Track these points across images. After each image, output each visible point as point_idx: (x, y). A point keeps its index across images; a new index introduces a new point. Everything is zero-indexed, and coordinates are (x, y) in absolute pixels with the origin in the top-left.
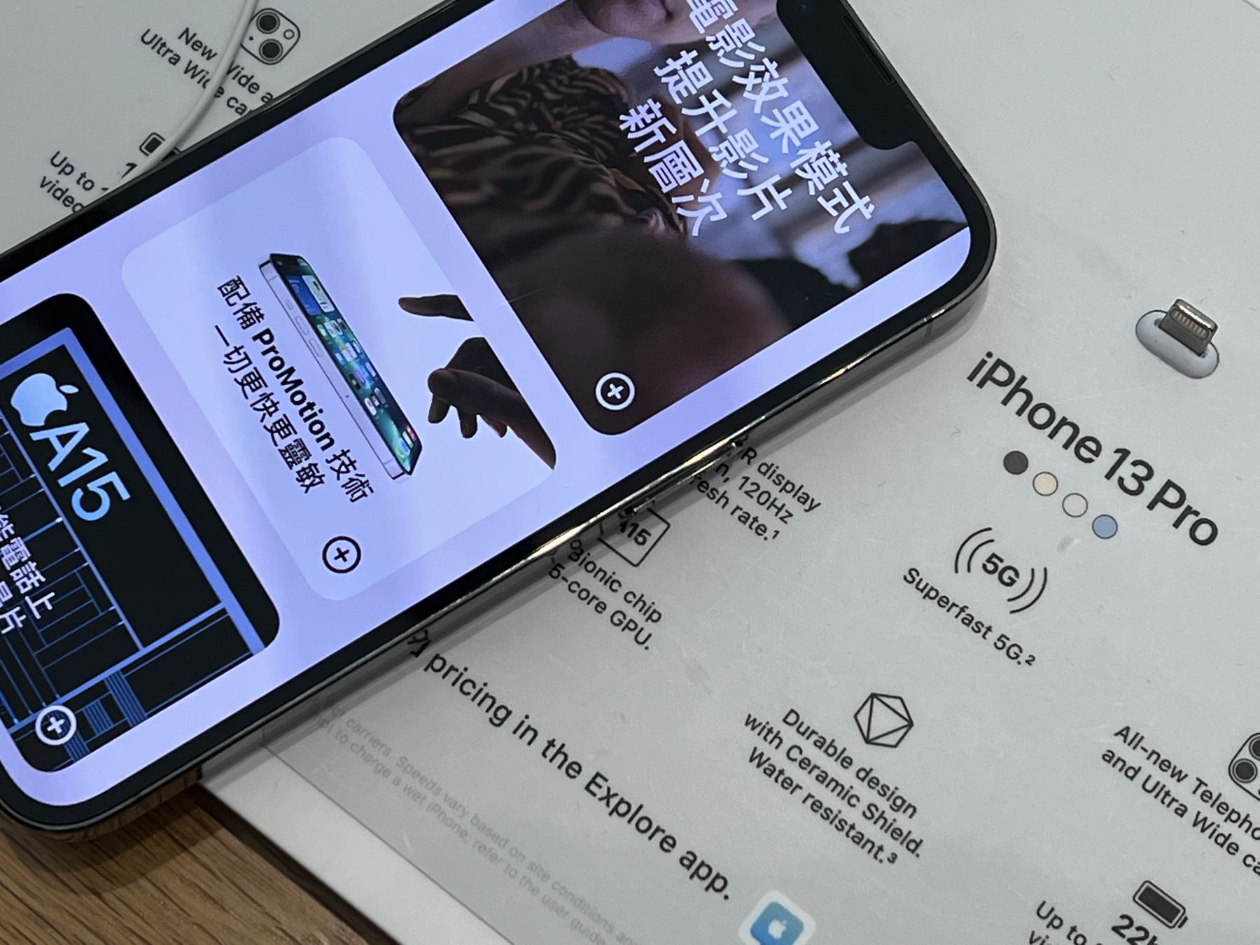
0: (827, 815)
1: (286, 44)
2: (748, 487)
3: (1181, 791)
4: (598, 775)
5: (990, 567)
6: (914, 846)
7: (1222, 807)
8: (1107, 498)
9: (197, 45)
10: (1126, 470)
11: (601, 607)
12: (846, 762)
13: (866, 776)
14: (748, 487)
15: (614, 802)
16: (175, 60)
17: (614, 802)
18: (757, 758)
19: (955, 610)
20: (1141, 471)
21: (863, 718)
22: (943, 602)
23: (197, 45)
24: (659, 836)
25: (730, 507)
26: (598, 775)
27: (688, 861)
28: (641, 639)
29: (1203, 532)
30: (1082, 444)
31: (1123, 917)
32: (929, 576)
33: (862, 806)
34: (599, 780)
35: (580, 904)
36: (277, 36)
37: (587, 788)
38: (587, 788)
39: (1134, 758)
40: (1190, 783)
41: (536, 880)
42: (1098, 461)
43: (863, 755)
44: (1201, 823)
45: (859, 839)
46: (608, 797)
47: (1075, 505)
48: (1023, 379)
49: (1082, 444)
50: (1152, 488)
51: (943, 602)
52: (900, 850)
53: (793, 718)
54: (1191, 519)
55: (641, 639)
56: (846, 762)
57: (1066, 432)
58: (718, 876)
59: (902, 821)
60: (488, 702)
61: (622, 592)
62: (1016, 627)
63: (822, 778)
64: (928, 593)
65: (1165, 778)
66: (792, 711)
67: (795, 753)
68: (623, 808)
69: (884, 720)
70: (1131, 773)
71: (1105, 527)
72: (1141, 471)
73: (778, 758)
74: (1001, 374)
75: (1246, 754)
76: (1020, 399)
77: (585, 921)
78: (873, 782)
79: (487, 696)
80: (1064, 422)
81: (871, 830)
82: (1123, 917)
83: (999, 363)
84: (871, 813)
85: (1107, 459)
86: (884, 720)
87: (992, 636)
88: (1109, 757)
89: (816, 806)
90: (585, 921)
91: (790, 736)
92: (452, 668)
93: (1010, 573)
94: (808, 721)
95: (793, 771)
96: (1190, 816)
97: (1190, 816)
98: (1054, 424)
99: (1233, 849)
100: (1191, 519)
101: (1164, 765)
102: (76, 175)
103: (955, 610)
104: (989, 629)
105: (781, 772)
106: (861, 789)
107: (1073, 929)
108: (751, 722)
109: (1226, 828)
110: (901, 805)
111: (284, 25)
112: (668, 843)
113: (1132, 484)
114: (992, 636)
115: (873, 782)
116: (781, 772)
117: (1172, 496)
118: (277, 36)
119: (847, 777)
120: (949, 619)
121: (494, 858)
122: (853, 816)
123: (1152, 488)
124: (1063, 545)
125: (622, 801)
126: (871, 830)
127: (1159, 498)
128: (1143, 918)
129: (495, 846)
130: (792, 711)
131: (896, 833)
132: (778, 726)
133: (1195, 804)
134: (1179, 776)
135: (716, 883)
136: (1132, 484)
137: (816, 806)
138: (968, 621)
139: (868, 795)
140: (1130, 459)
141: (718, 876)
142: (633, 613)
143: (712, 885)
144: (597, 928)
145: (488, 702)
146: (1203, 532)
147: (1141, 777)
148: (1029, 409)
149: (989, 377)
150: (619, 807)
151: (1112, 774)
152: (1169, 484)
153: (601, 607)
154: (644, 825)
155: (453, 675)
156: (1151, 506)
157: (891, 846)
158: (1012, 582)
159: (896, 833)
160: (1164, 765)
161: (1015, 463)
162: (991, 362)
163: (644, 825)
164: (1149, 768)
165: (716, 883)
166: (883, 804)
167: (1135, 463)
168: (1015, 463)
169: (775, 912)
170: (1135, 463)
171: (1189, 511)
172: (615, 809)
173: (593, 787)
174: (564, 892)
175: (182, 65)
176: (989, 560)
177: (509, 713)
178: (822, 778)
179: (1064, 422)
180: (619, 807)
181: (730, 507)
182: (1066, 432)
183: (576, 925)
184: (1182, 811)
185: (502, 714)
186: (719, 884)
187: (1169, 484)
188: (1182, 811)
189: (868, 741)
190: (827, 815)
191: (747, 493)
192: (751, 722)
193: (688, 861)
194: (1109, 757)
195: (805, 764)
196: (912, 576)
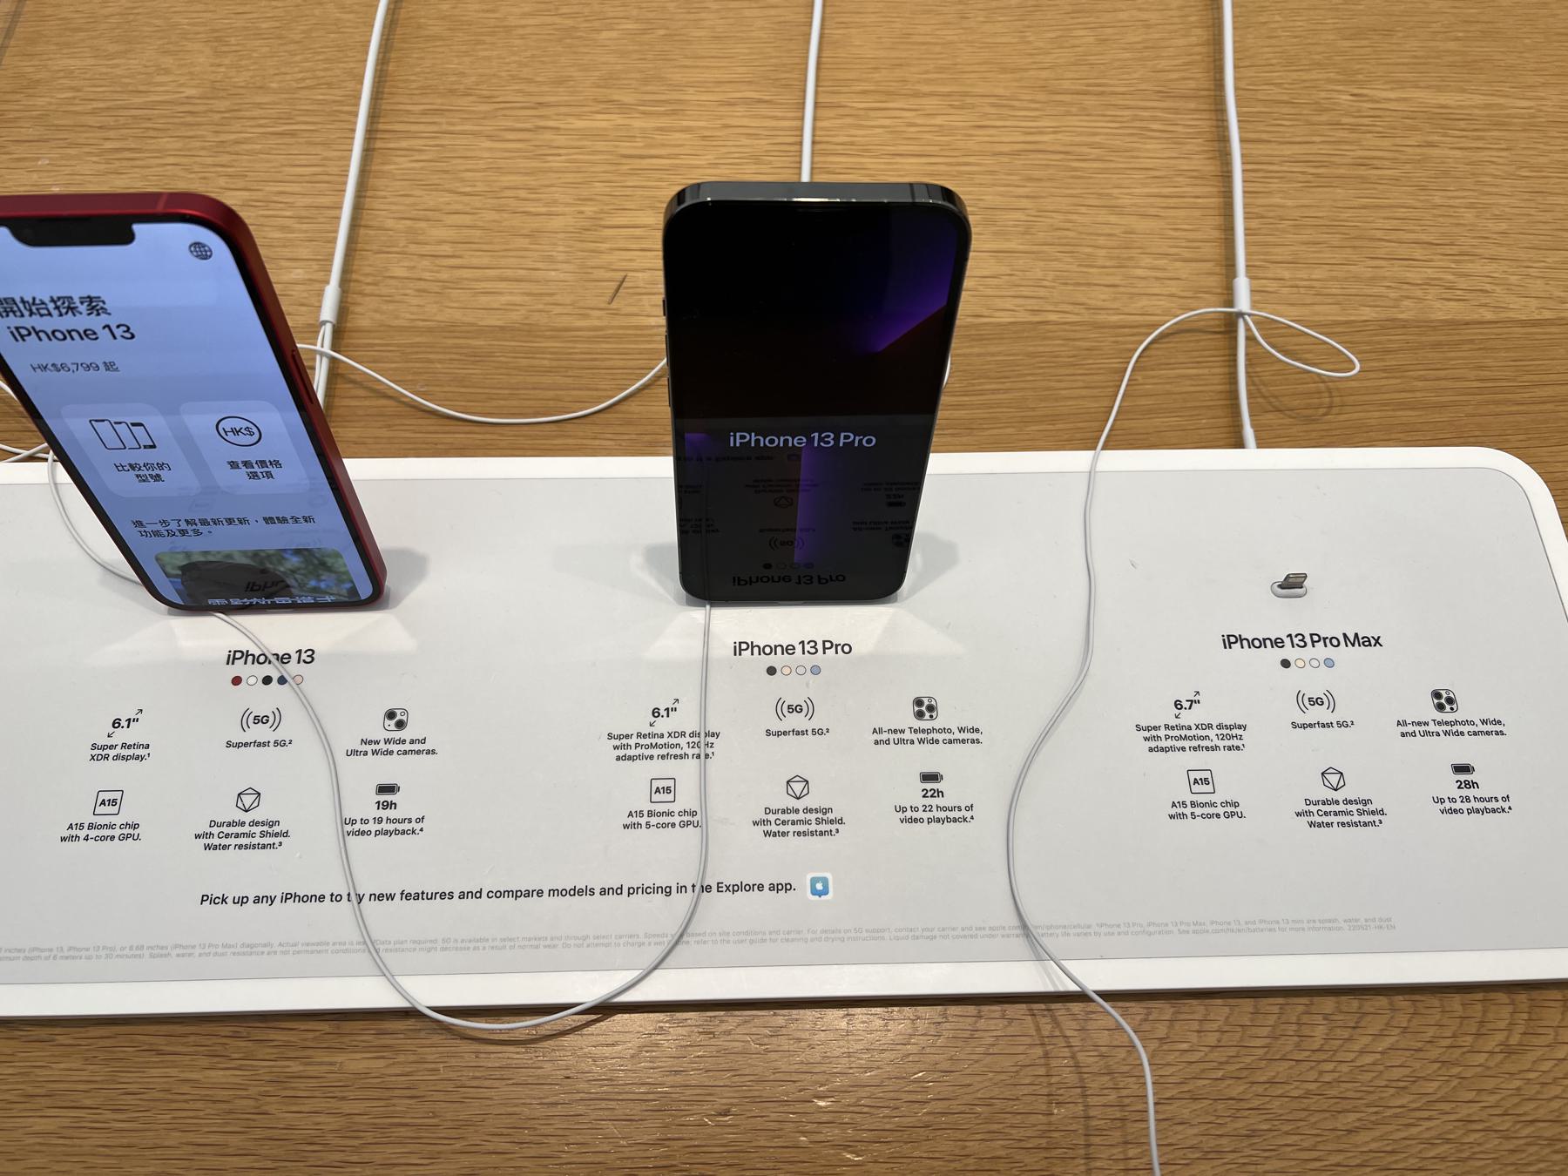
0: (805, 834)
1: (404, 718)
2: (691, 745)
3: (907, 735)
4: (718, 883)
5: (791, 710)
6: (841, 821)
7: (923, 731)
8: (809, 661)
9: (370, 742)
10: (807, 647)
11: (673, 825)
12: (797, 811)
13: (808, 810)
14: (691, 745)
15: (731, 888)
16: (366, 754)
17: (731, 888)
18: (767, 834)
19: (791, 733)
20: (812, 644)
21: (790, 792)
22: (785, 733)
23: (370, 742)
24: (756, 887)
25: (690, 757)
26: (718, 883)
27: (772, 887)
28: (696, 825)
29: (847, 649)
30: (787, 649)
31: (923, 791)
32: (774, 729)
33: (814, 822)
34: (720, 885)
35: (747, 933)
36: (398, 717)
37: (718, 891)
38: (718, 891)
39: (884, 736)
40: (908, 731)
41: (725, 938)
42: (796, 651)
43: (800, 804)
44: (921, 741)
45: (822, 834)
46: (728, 888)
47: (801, 670)
48: (752, 643)
49: (787, 649)
50: (820, 647)
51: (785, 733)
52: (838, 826)
53: (768, 811)
54: (839, 648)
55: (696, 825)
56: (797, 811)
57: (779, 649)
58: (786, 885)
59: (830, 816)
60: (660, 889)
61: (676, 814)
62: (816, 723)
63: (793, 823)
64: (778, 734)
65: (899, 735)
66: (766, 808)
67: (778, 822)
68: (736, 888)
69: (798, 787)
70: (887, 742)
71: (816, 670)
72: (812, 644)
73: (774, 828)
74: (744, 646)
75: (916, 709)
76: (756, 650)
77: (754, 937)
78: (811, 811)
79: (658, 888)
80: (776, 647)
81: (823, 827)
82: (923, 791)
83: (740, 643)
84: (818, 821)
85: (799, 648)
86: (798, 787)
87: (810, 732)
88: (877, 742)
89: (799, 834)
90: (754, 937)
91: (772, 817)
92: (638, 888)
93: (798, 708)
94: (773, 807)
95: (782, 828)
96: (916, 742)
97: (916, 742)
98: (774, 650)
99: (937, 741)
100: (839, 648)
101: (895, 731)
102: (359, 821)
103: (791, 733)
104: (807, 731)
105: (779, 832)
106: (809, 816)
107: (911, 807)
108: (755, 823)
109: (930, 736)
110: (826, 811)
111: (398, 712)
112: (760, 887)
113: (813, 650)
114: (810, 732)
115: (811, 811)
116: (779, 832)
117: (828, 645)
118: (398, 717)
119: (801, 816)
120: (791, 737)
121: (705, 942)
122: (813, 827)
123: (820, 647)
124: (807, 685)
125: (733, 886)
126: (823, 827)
127: (825, 649)
128: (929, 786)
129: (702, 938)
130: (766, 808)
131: (832, 822)
132: (765, 817)
133: (914, 737)
134: (902, 731)
135: (787, 887)
136: (813, 650)
137: (799, 834)
138: (798, 733)
139: (813, 816)
140: (806, 643)
141: (786, 885)
142: (686, 818)
143: (786, 889)
144: (760, 937)
145: (660, 889)
146: (847, 649)
147: (891, 741)
148: (761, 651)
149: (741, 650)
150: (734, 889)
151: (882, 747)
152: (824, 642)
153: (673, 825)
154: (747, 888)
155: (640, 890)
156: (824, 653)
157: (833, 827)
158: (802, 710)
159: (832, 822)
160: (895, 731)
161: (771, 671)
162: (737, 645)
163: (747, 888)
164: (892, 736)
165: (787, 887)
166: (820, 815)
167: (808, 643)
168: (771, 671)
169: (814, 881)
170: (808, 643)
171: (837, 646)
172: (733, 890)
173: (720, 889)
174: (739, 933)
175: (370, 753)
176: (789, 708)
177: (670, 887)
178: (793, 823)
179: (776, 647)
180: (734, 889)
181: (690, 757)
182: (779, 649)
183: (752, 942)
184: (912, 742)
185: (668, 890)
186: (788, 887)
187: (824, 642)
188: (912, 742)
189: (798, 798)
190: (805, 834)
191: (693, 747)
192: (755, 823)
193: (772, 887)
194: (877, 742)
195: (784, 823)
196: (768, 733)
